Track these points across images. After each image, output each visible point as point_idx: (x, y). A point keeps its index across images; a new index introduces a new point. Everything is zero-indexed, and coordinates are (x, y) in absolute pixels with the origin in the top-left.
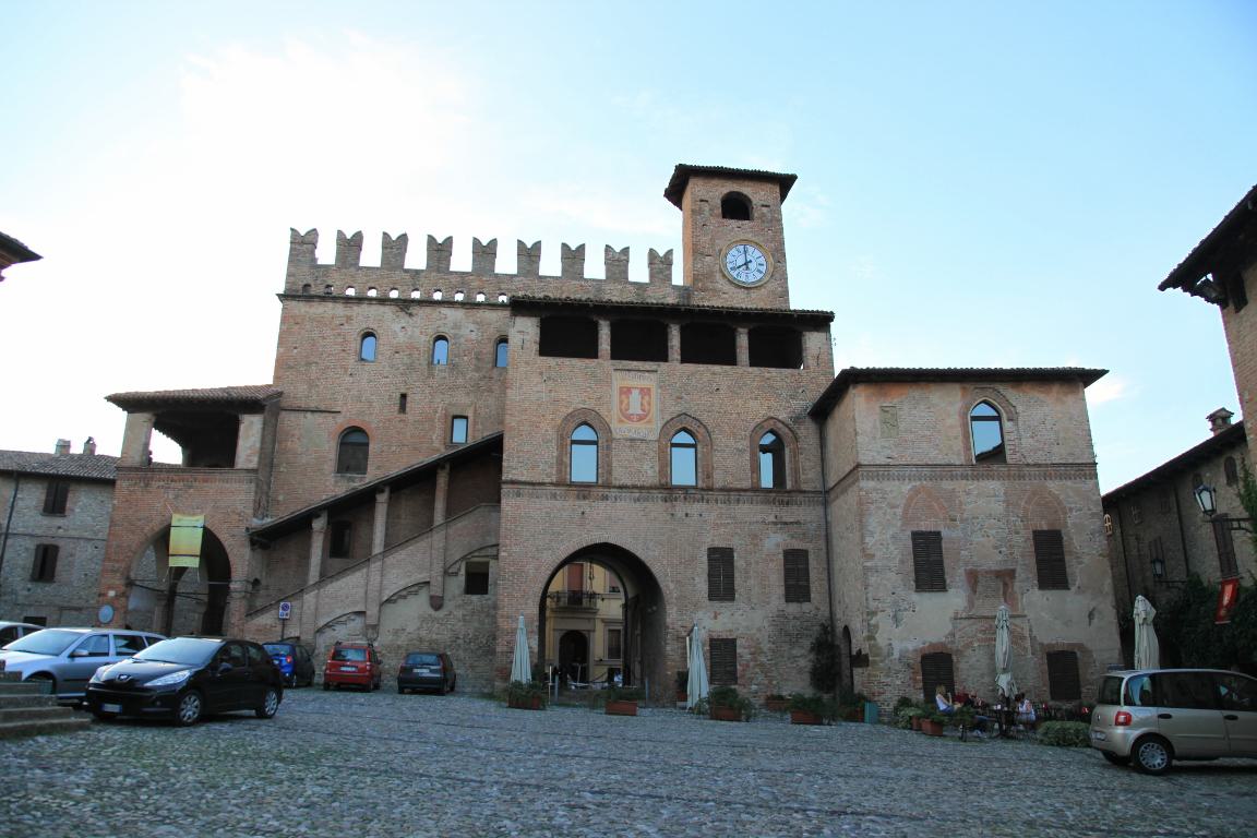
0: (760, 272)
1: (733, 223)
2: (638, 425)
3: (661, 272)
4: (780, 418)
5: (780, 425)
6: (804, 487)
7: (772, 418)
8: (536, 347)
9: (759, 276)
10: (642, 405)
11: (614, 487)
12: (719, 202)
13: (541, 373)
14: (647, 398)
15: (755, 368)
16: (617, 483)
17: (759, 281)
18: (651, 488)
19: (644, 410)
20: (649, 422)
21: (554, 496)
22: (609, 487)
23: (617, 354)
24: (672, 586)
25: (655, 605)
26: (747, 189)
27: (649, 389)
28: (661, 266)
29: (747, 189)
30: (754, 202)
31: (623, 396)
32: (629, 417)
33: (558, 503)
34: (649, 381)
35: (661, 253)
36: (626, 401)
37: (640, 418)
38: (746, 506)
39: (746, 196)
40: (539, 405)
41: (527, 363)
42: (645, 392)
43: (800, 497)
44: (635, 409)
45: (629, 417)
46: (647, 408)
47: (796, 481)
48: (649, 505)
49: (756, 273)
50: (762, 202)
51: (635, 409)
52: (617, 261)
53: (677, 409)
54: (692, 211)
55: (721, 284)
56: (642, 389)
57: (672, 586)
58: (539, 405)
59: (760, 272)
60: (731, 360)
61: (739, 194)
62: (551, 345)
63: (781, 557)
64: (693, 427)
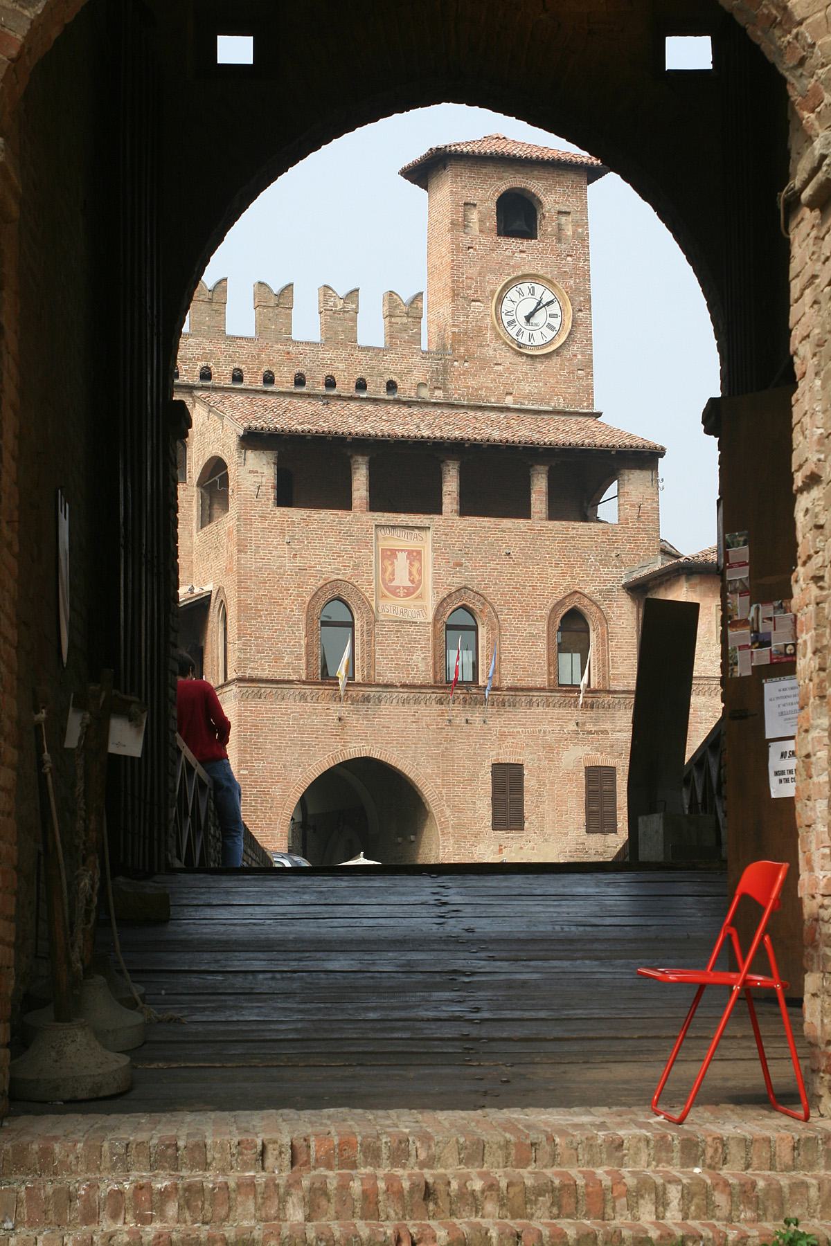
0: (551, 327)
1: (516, 244)
2: (402, 601)
3: (405, 328)
4: (586, 591)
5: (586, 601)
6: (615, 686)
7: (576, 592)
8: (272, 494)
9: (550, 334)
10: (410, 573)
11: (378, 685)
12: (493, 206)
13: (282, 531)
14: (416, 564)
15: (557, 523)
16: (381, 680)
17: (551, 342)
18: (422, 686)
19: (412, 581)
20: (420, 597)
21: (303, 698)
22: (370, 685)
23: (378, 503)
24: (448, 812)
25: (415, 834)
26: (535, 185)
27: (419, 553)
28: (405, 320)
29: (535, 185)
30: (547, 207)
31: (387, 563)
32: (394, 591)
33: (308, 706)
34: (425, 543)
35: (406, 296)
36: (390, 568)
37: (409, 592)
38: (541, 709)
39: (534, 195)
40: (281, 576)
41: (263, 517)
42: (414, 556)
43: (608, 699)
44: (402, 580)
45: (394, 591)
46: (417, 578)
47: (604, 677)
48: (422, 708)
49: (545, 330)
50: (558, 207)
51: (402, 579)
52: (340, 312)
53: (458, 581)
54: (452, 223)
55: (492, 349)
56: (410, 552)
57: (448, 812)
58: (281, 576)
59: (551, 327)
60: (523, 511)
61: (523, 190)
62: (288, 493)
63: (582, 775)
64: (476, 607)
